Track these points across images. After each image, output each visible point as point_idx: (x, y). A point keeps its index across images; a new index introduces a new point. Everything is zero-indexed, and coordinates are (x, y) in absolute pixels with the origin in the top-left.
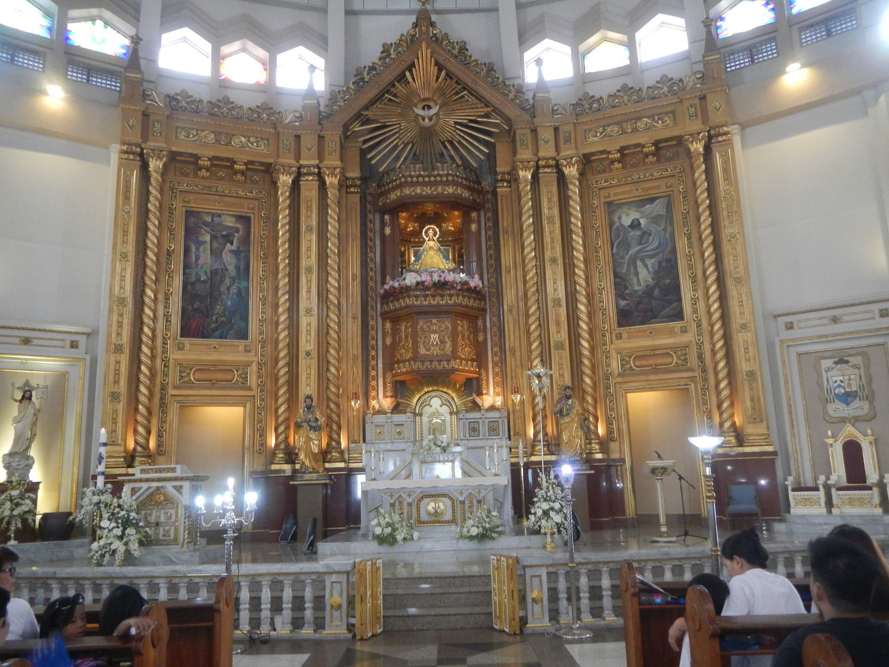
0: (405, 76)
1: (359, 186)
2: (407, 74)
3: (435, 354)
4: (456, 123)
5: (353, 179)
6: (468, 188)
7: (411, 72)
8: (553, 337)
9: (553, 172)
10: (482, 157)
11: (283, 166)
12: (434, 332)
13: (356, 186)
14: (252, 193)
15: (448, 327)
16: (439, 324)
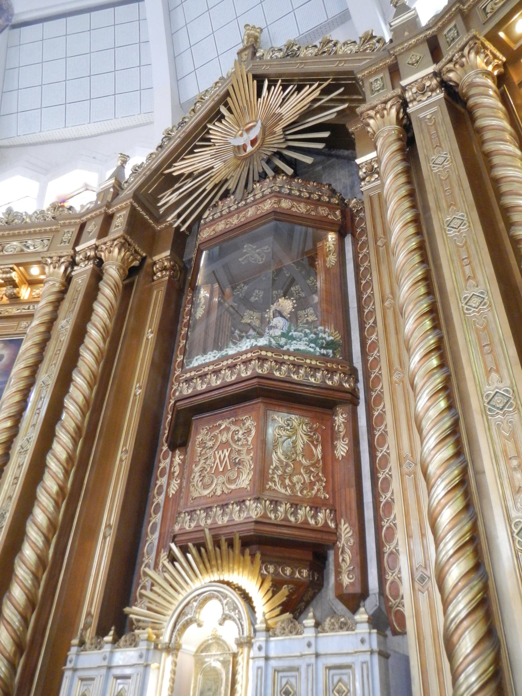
0: (219, 111)
1: (172, 268)
2: (223, 110)
3: (219, 493)
4: (285, 129)
5: (162, 261)
6: (308, 200)
7: (226, 105)
8: (478, 386)
9: (438, 94)
10: (320, 146)
11: (51, 258)
12: (225, 445)
13: (165, 269)
14: (29, 309)
15: (251, 430)
16: (233, 428)
